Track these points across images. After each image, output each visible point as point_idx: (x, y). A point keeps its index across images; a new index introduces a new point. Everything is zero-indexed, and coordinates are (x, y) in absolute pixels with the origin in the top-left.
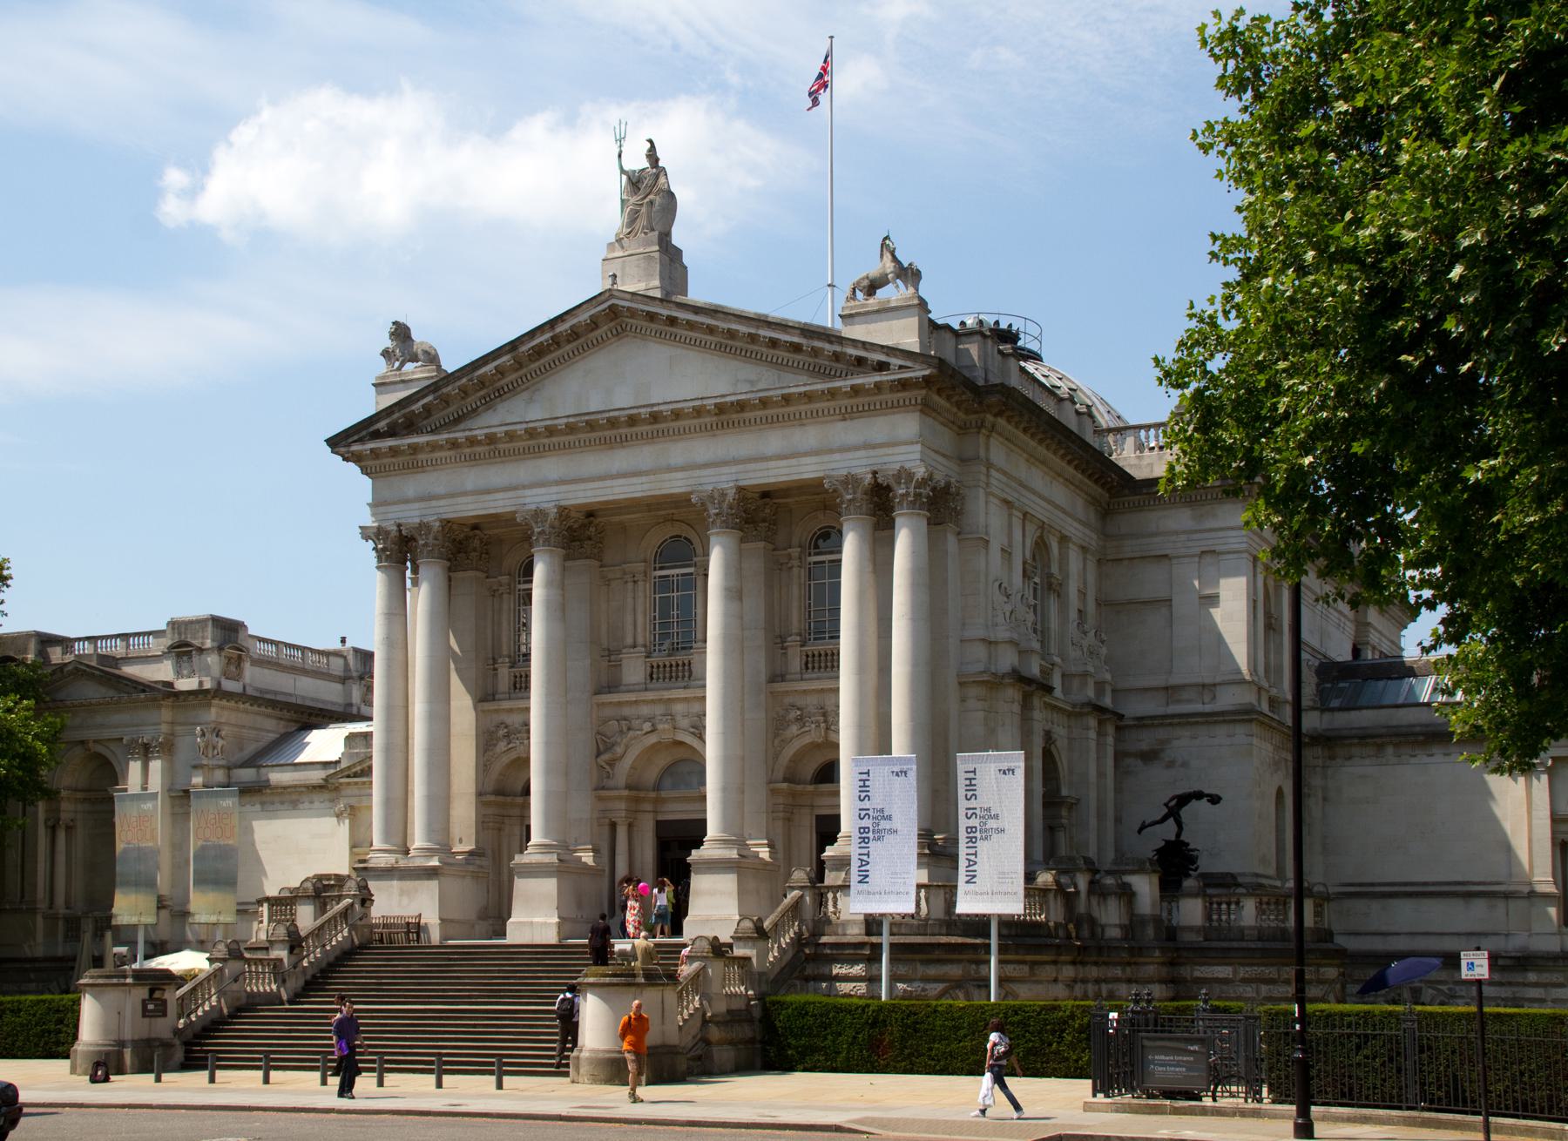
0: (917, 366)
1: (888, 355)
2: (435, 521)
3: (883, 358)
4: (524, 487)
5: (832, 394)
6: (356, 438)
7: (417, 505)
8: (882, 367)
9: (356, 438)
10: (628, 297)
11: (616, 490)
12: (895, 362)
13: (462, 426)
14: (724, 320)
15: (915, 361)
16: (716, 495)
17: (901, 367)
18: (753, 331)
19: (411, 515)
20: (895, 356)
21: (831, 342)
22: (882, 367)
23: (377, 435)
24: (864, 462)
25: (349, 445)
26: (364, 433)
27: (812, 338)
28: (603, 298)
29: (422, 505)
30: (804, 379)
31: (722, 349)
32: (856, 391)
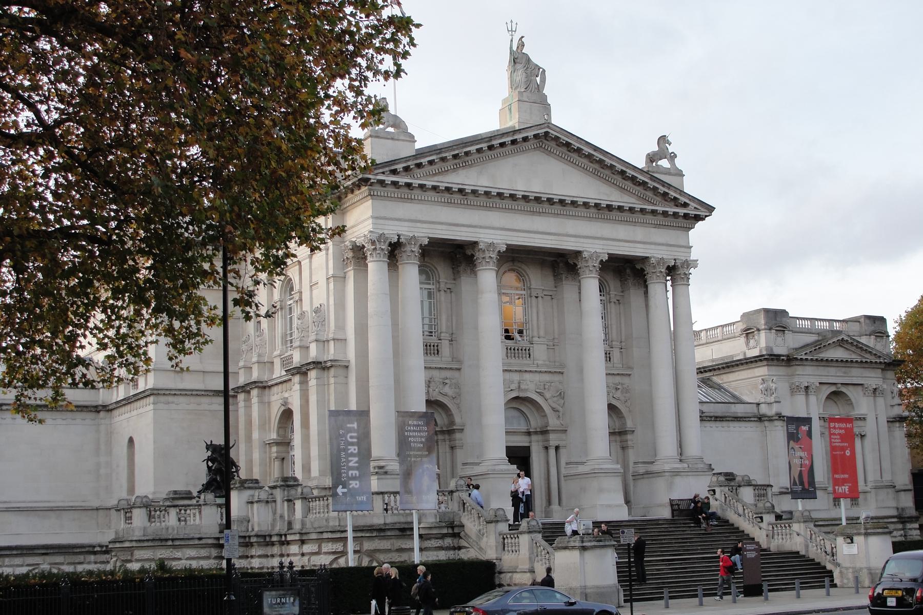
0: (703, 210)
1: (690, 200)
2: (503, 244)
3: (687, 201)
4: (481, 227)
5: (654, 212)
6: (381, 171)
7: (406, 224)
8: (685, 205)
9: (381, 171)
10: (559, 130)
11: (537, 241)
12: (693, 204)
13: (436, 178)
14: (610, 159)
15: (702, 206)
16: (595, 255)
17: (695, 208)
18: (624, 169)
19: (405, 230)
20: (694, 202)
21: (663, 186)
22: (685, 205)
23: (394, 172)
24: (502, 237)
25: (377, 174)
26: (387, 169)
27: (654, 181)
28: (543, 126)
29: (410, 224)
30: (633, 200)
31: (595, 174)
32: (665, 214)
